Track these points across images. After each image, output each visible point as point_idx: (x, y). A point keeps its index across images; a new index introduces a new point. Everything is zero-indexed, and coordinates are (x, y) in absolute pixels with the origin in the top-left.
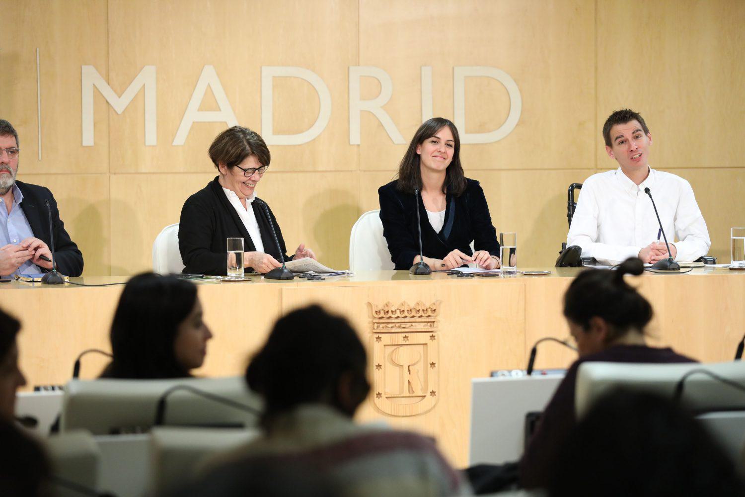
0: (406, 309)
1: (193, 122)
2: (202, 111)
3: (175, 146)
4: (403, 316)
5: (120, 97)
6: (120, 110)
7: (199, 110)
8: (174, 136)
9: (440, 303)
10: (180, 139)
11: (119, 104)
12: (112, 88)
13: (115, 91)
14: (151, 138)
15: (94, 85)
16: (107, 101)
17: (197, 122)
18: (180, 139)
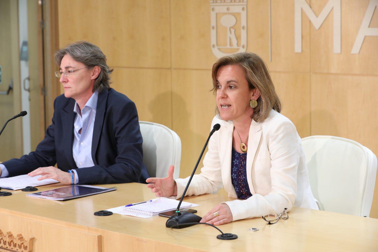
0: (8, 240)
1: (365, 36)
2: (372, 27)
3: (353, 54)
4: (5, 247)
5: (317, 16)
6: (317, 26)
7: (369, 27)
8: (352, 45)
9: (32, 240)
10: (356, 49)
11: (317, 22)
12: (313, 11)
13: (315, 13)
14: (337, 48)
15: (302, 9)
16: (310, 21)
17: (369, 36)
18: (356, 49)
